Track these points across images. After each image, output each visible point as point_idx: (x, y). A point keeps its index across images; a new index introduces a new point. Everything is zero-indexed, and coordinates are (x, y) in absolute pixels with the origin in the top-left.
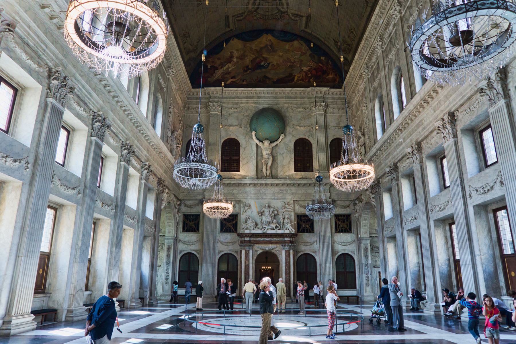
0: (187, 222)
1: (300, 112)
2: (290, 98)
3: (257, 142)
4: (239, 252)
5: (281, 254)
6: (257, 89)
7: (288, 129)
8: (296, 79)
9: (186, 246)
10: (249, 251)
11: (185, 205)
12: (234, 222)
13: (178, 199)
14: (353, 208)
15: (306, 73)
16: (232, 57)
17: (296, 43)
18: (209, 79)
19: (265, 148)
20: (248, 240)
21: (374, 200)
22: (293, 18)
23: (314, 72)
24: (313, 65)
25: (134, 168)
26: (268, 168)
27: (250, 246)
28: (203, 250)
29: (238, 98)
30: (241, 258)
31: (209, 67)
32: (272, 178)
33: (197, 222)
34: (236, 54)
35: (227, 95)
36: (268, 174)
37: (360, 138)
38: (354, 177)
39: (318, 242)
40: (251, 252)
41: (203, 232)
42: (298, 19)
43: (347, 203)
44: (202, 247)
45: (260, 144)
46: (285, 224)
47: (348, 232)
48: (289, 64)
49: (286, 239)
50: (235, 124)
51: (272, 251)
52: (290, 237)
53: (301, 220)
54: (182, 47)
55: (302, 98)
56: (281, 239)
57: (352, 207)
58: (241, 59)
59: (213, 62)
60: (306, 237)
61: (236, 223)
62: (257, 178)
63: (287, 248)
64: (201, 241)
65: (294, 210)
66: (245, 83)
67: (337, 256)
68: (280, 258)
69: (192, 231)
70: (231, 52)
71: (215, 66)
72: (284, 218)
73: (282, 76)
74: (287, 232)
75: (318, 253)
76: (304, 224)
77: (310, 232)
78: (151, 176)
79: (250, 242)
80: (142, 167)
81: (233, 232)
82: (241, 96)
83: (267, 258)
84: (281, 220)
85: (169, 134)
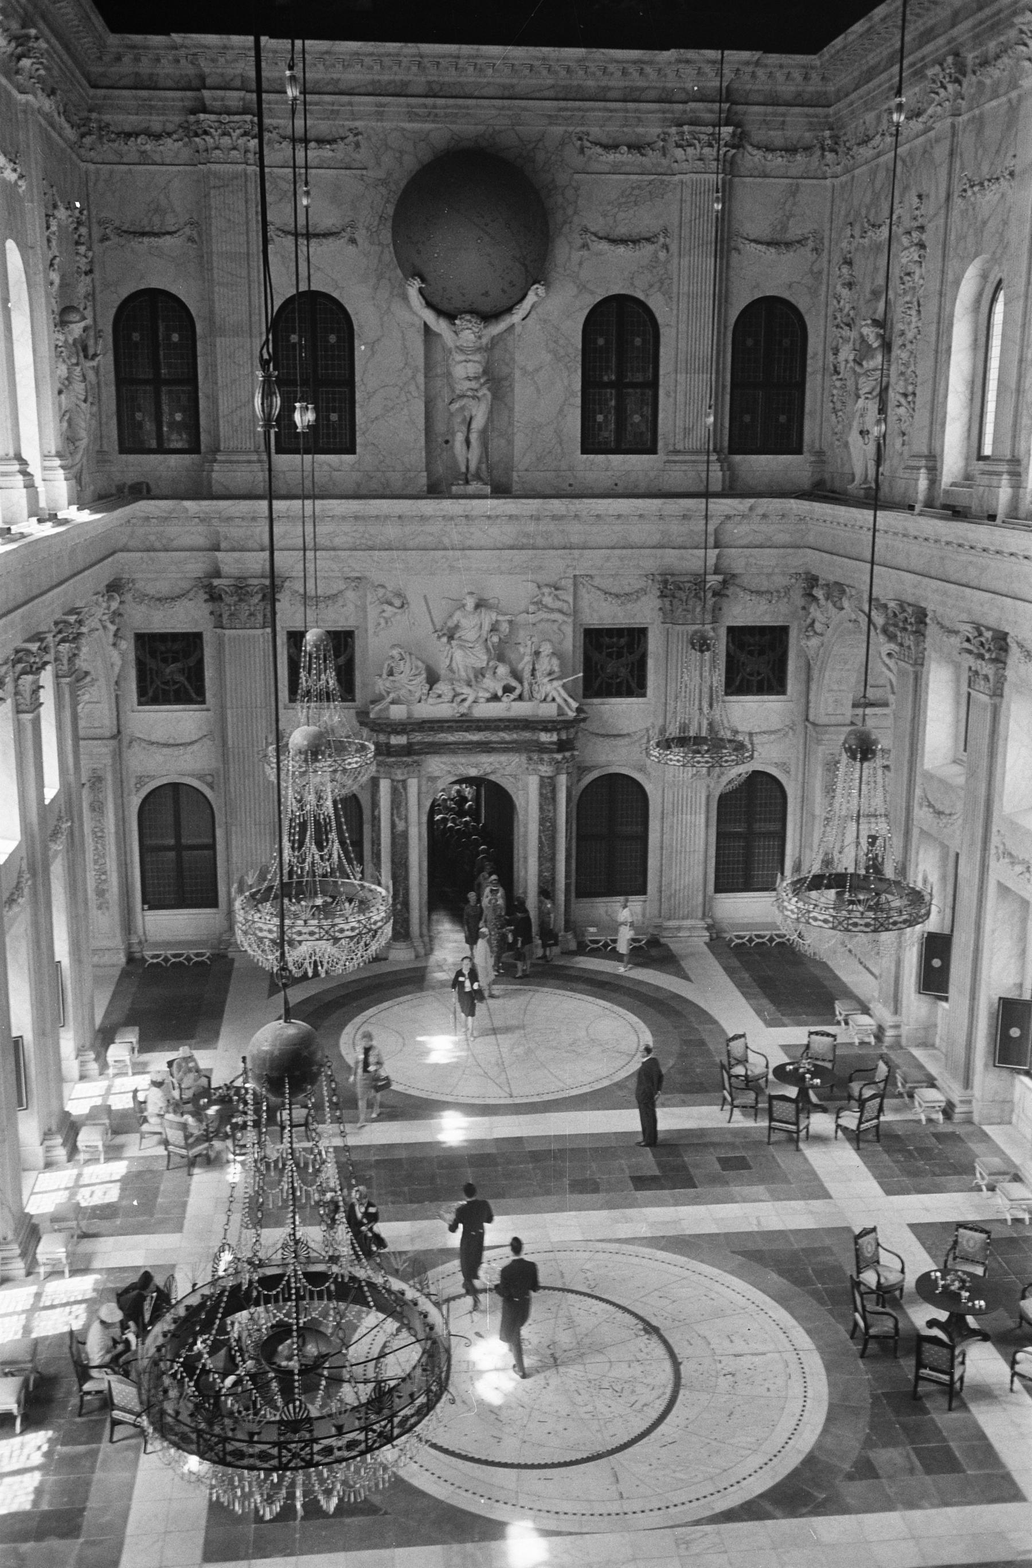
0: (151, 664)
3: (429, 316)
5: (525, 788)
6: (426, 48)
10: (404, 781)
11: (142, 597)
19: (460, 349)
20: (405, 743)
26: (474, 437)
28: (226, 771)
30: (375, 804)
33: (192, 662)
36: (473, 466)
40: (413, 784)
41: (223, 707)
44: (225, 761)
45: (440, 326)
46: (538, 674)
49: (544, 737)
51: (492, 778)
56: (527, 735)
63: (546, 770)
64: (219, 733)
65: (576, 612)
68: (519, 801)
69: (178, 701)
74: (548, 711)
76: (612, 661)
77: (630, 694)
84: (525, 666)
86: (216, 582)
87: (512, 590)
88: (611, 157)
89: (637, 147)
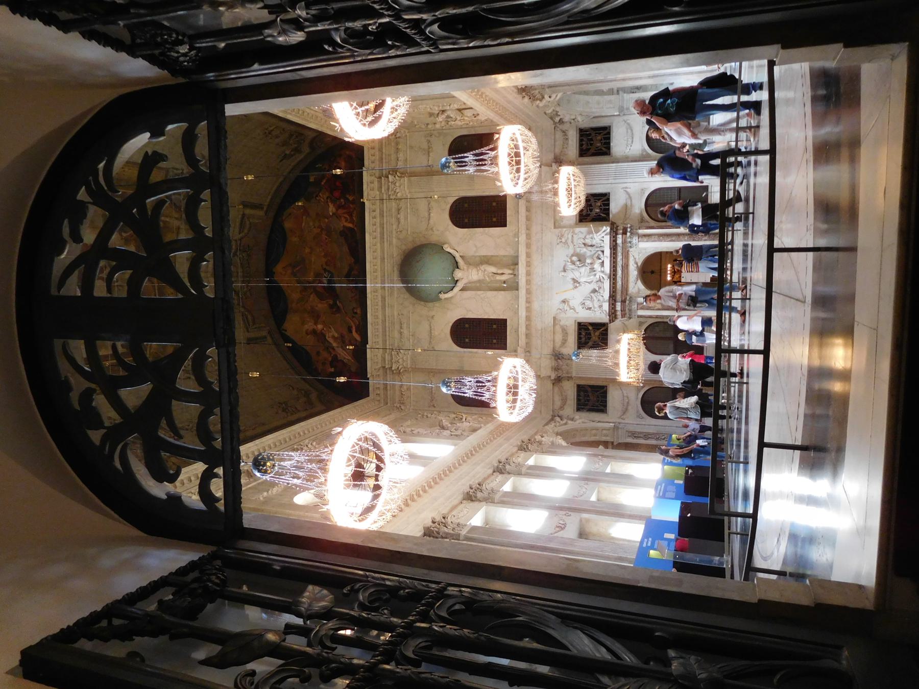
1: (406, 218)
2: (382, 234)
3: (456, 290)
4: (641, 319)
5: (645, 249)
7: (434, 239)
8: (350, 225)
9: (630, 408)
11: (562, 408)
12: (590, 328)
13: (552, 419)
14: (568, 125)
15: (339, 207)
16: (314, 332)
17: (288, 225)
18: (353, 369)
21: (554, 96)
22: (246, 231)
23: (337, 194)
24: (323, 196)
25: (503, 483)
27: (630, 301)
29: (384, 321)
30: (650, 317)
31: (333, 370)
32: (517, 264)
33: (589, 389)
34: (310, 326)
35: (380, 340)
36: (511, 272)
37: (448, 117)
38: (517, 155)
39: (625, 185)
42: (248, 223)
43: (559, 135)
45: (460, 285)
47: (609, 133)
48: (324, 236)
49: (619, 241)
50: (427, 327)
51: (639, 264)
52: (617, 234)
53: (588, 215)
54: (303, 414)
55: (382, 215)
56: (619, 249)
57: (564, 127)
58: (318, 317)
59: (324, 364)
60: (615, 207)
61: (592, 324)
62: (517, 290)
66: (359, 311)
67: (650, 151)
69: (606, 397)
70: (307, 334)
71: (330, 359)
72: (585, 244)
73: (345, 249)
74: (607, 239)
75: (645, 186)
77: (608, 200)
78: (516, 461)
79: (623, 302)
80: (501, 473)
81: (607, 330)
82: (380, 317)
83: (652, 272)
85: (446, 433)
86: (553, 378)
87: (561, 255)
88: (402, 221)
89: (399, 210)
